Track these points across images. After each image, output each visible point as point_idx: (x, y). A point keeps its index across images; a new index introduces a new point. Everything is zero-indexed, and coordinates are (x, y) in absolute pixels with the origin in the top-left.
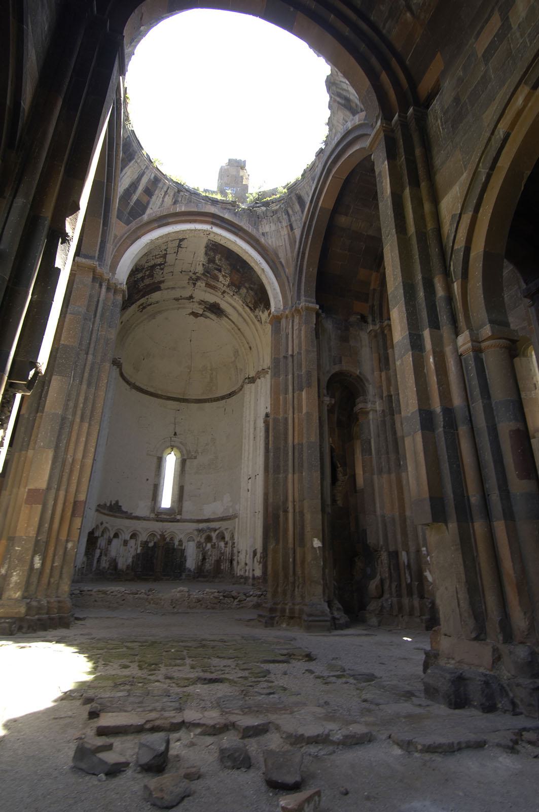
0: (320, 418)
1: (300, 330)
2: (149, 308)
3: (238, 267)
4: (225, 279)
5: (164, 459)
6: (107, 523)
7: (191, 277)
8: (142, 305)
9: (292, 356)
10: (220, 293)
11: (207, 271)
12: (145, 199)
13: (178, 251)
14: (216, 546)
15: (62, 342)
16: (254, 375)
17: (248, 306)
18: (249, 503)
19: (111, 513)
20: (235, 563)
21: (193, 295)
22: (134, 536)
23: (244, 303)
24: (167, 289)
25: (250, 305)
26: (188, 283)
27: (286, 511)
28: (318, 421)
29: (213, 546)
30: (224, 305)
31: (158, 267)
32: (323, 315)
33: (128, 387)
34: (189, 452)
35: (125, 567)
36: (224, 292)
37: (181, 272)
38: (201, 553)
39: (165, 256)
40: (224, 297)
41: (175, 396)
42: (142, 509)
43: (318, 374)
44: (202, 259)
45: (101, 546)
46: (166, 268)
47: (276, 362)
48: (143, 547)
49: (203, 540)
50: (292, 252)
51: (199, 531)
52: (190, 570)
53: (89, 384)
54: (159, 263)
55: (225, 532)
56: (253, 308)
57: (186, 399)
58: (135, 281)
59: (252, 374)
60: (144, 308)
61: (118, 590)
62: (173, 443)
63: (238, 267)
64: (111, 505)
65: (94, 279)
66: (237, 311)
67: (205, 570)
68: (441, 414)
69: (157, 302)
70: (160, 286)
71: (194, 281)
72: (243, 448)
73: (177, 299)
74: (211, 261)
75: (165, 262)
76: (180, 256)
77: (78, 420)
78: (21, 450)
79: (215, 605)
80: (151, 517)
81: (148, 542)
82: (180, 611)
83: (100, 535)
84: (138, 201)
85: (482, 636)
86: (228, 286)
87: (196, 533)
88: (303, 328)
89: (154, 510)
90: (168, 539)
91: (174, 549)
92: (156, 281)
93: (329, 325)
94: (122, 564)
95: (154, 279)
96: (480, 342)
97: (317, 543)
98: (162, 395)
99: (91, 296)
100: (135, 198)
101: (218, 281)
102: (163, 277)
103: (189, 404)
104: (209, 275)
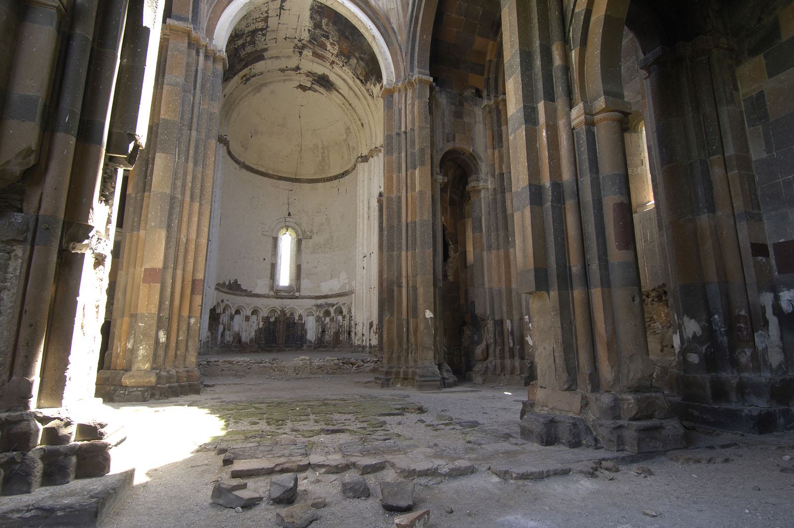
0: (433, 196)
1: (413, 105)
2: (252, 79)
3: (347, 34)
4: (333, 48)
5: (279, 239)
6: (227, 300)
7: (296, 45)
8: (245, 76)
9: (405, 133)
10: (329, 64)
11: (313, 39)
13: (280, 14)
14: (335, 319)
15: (162, 117)
16: (367, 154)
17: (358, 78)
18: (365, 280)
19: (231, 292)
20: (353, 334)
21: (300, 65)
22: (255, 312)
23: (354, 75)
24: (270, 58)
25: (361, 77)
26: (294, 51)
27: (400, 286)
28: (431, 200)
29: (332, 320)
30: (333, 78)
31: (260, 33)
32: (437, 89)
33: (237, 166)
34: (304, 232)
35: (248, 340)
36: (333, 62)
37: (286, 40)
38: (321, 326)
39: (266, 20)
40: (333, 68)
41: (286, 176)
42: (261, 287)
43: (432, 152)
44: (308, 24)
45: (224, 322)
46: (268, 34)
47: (389, 139)
48: (265, 322)
49: (321, 315)
50: (405, 17)
51: (318, 306)
52: (310, 342)
53: (196, 163)
54: (260, 27)
55: (343, 307)
56: (364, 81)
57: (297, 179)
58: (235, 48)
59: (365, 152)
60: (248, 80)
61: (244, 360)
62: (287, 224)
63: (347, 34)
64: (230, 283)
65: (190, 45)
66: (348, 84)
67: (325, 341)
68: (550, 189)
69: (262, 73)
70: (263, 55)
71: (300, 49)
72: (358, 226)
73: (282, 70)
74: (317, 26)
75: (267, 27)
76: (284, 19)
77: (188, 199)
78: (132, 231)
79: (335, 371)
80: (270, 294)
81: (269, 317)
82: (303, 376)
83: (222, 312)
85: (573, 387)
86: (337, 56)
87: (315, 308)
88: (416, 102)
89: (273, 287)
90: (288, 315)
91: (294, 323)
92: (258, 49)
93: (443, 100)
94: (245, 338)
95: (256, 46)
96: (593, 115)
97: (429, 314)
98: (274, 175)
99: (188, 65)
101: (326, 50)
102: (266, 44)
103: (302, 184)
104: (316, 42)
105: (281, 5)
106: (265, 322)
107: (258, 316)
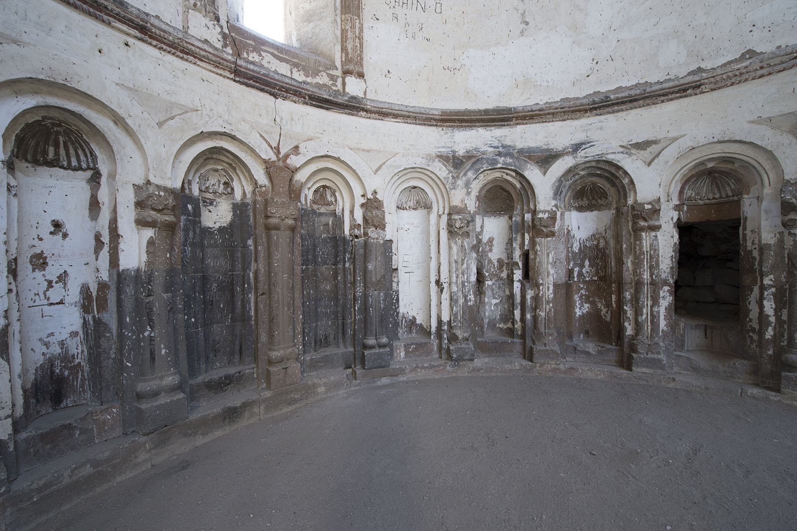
48: (171, 228)
51: (456, 162)
81: (195, 202)
87: (442, 171)
90: (308, 194)
91: (338, 243)
106: (171, 228)
107: (95, 180)
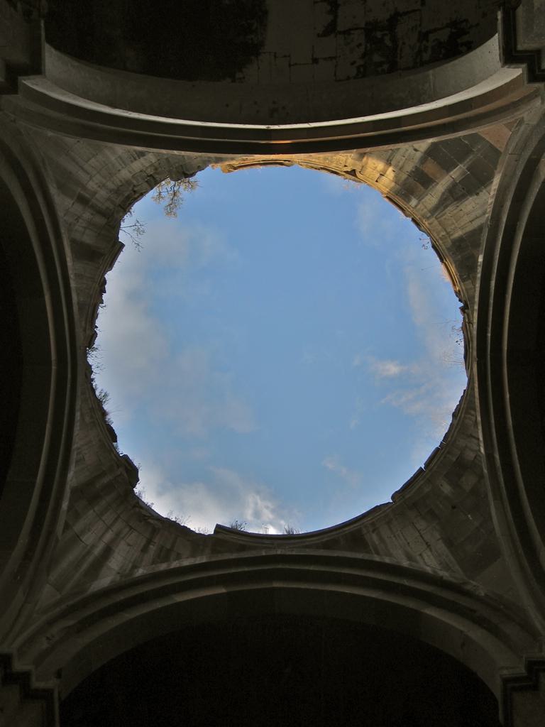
12: (430, 168)
84: (447, 167)
100: (456, 173)
105: (336, 17)
